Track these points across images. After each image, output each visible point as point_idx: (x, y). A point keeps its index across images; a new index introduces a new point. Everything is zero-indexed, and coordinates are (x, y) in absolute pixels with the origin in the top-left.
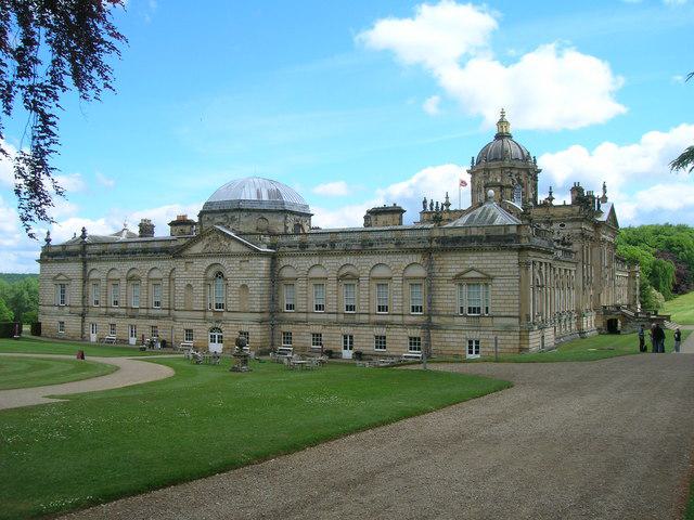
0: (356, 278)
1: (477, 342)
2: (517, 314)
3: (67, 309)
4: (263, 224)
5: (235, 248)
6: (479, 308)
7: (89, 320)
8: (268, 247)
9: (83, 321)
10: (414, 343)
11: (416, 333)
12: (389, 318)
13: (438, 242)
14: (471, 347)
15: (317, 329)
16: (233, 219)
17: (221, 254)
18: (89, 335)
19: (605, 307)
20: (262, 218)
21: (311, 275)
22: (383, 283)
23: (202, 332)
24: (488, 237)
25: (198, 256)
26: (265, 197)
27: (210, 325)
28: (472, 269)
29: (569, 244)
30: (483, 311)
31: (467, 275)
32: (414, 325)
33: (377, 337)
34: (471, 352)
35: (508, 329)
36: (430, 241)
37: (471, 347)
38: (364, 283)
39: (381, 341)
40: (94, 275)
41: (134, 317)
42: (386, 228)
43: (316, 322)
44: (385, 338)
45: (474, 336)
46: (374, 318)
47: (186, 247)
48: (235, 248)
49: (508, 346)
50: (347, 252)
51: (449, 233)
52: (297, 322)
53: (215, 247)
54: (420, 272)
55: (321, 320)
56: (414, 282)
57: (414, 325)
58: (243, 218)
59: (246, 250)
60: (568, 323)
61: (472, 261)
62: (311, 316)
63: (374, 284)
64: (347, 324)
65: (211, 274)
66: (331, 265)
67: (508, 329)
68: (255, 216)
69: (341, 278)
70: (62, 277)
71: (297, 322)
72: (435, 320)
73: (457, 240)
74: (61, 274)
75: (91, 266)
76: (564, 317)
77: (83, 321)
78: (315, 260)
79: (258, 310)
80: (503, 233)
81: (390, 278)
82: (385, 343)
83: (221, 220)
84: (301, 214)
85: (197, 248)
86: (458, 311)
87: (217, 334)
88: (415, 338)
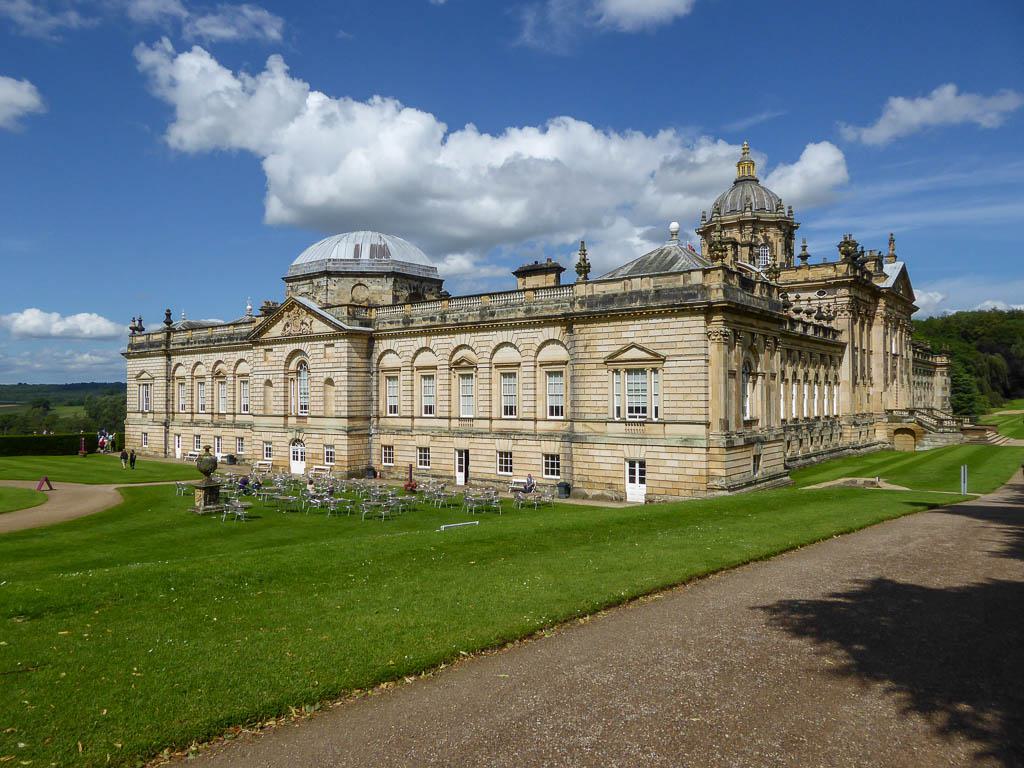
0: (472, 366)
1: (642, 464)
2: (702, 418)
3: (150, 416)
4: (362, 294)
5: (319, 327)
6: (644, 410)
7: (174, 429)
8: (361, 325)
9: (167, 432)
10: (552, 462)
11: (553, 447)
12: (518, 425)
13: (582, 304)
15: (424, 441)
18: (174, 450)
19: (891, 411)
21: (417, 363)
22: (509, 371)
23: (281, 442)
24: (657, 291)
25: (276, 341)
26: (365, 255)
27: (290, 436)
28: (634, 346)
29: (830, 319)
30: (650, 414)
31: (620, 357)
32: (550, 436)
33: (501, 454)
35: (687, 443)
36: (572, 304)
37: (632, 472)
38: (483, 372)
39: (506, 460)
40: (180, 372)
41: (217, 425)
43: (423, 431)
44: (511, 454)
45: (638, 453)
46: (497, 425)
47: (264, 329)
48: (319, 327)
49: (688, 471)
52: (399, 431)
53: (293, 330)
54: (555, 353)
55: (432, 429)
56: (554, 370)
57: (550, 436)
58: (334, 285)
60: (826, 434)
61: (633, 331)
62: (417, 422)
63: (496, 373)
65: (293, 366)
66: (443, 344)
67: (687, 443)
68: (349, 282)
69: (457, 365)
70: (144, 376)
71: (399, 431)
72: (579, 428)
73: (610, 299)
74: (143, 372)
75: (176, 359)
76: (819, 425)
77: (167, 432)
78: (421, 342)
79: (345, 414)
80: (680, 284)
81: (519, 365)
83: (305, 289)
84: (422, 280)
85: (276, 331)
86: (612, 414)
87: (299, 448)
88: (553, 457)
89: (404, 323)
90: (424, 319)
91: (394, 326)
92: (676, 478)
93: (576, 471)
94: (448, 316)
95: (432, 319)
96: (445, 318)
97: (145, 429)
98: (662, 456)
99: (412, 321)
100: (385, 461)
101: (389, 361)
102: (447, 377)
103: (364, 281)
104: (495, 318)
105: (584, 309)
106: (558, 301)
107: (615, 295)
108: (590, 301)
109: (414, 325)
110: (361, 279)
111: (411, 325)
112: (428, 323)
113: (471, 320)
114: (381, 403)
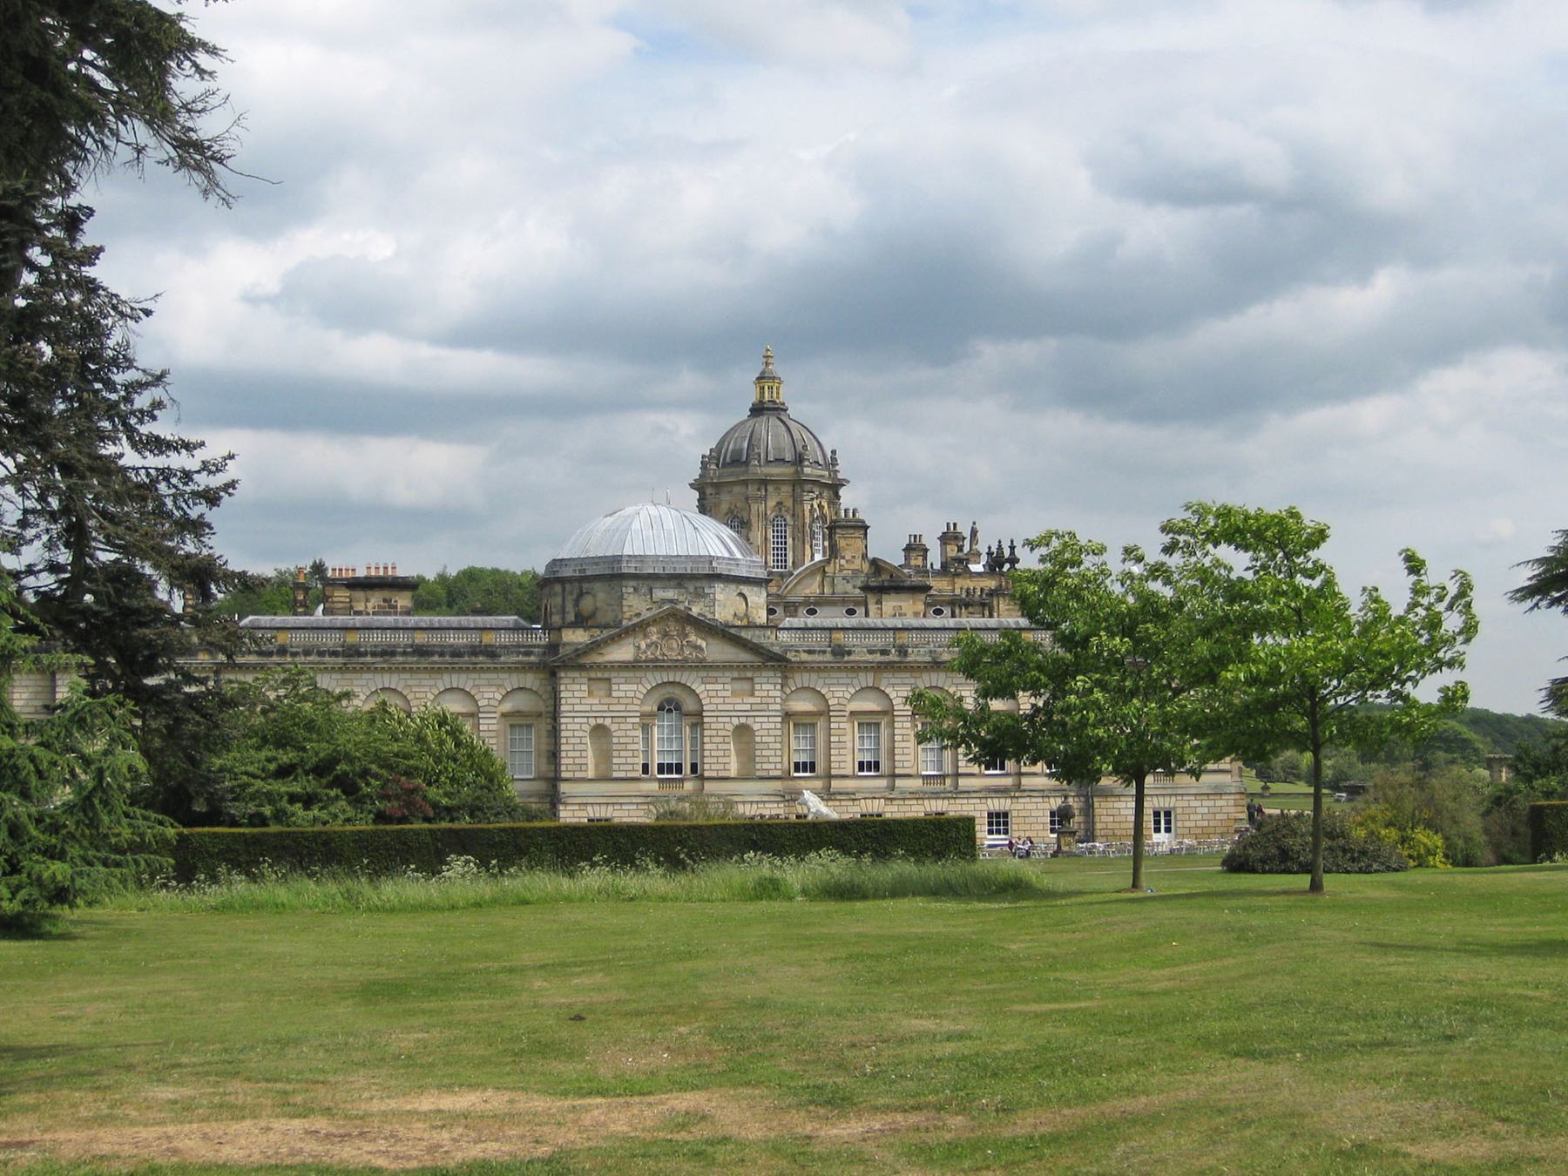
1: (1168, 814)
14: (1157, 822)
17: (682, 665)
34: (1157, 830)
37: (1157, 822)
47: (595, 646)
48: (715, 650)
64: (936, 795)
82: (1006, 823)
83: (670, 594)
85: (623, 652)
89: (834, 653)
90: (871, 652)
91: (816, 657)
92: (1205, 823)
93: (1098, 826)
95: (884, 652)
96: (906, 654)
98: (1194, 804)
99: (849, 653)
101: (802, 705)
103: (745, 589)
109: (852, 658)
112: (878, 658)
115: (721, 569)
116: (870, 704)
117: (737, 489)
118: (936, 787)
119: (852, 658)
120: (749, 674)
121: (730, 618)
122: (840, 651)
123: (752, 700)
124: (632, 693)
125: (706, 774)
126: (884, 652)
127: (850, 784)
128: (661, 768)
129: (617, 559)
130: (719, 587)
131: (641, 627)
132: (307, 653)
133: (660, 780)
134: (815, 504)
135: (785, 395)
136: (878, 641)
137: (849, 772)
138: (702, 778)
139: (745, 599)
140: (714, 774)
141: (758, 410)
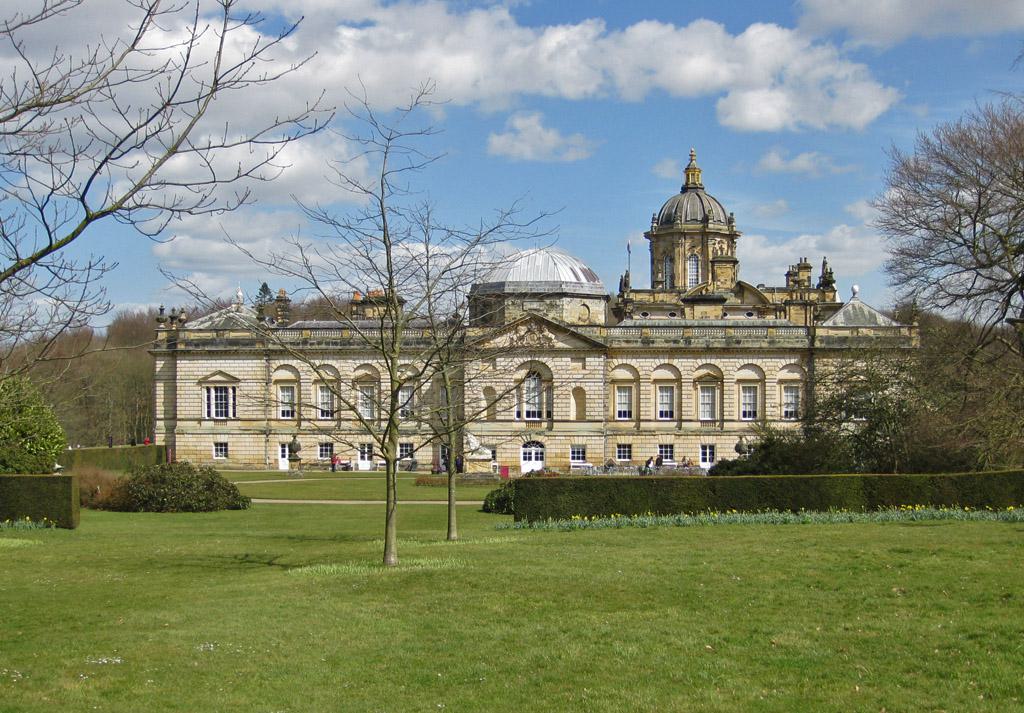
13: (821, 341)
15: (668, 440)
16: (552, 306)
17: (541, 351)
20: (584, 305)
42: (707, 323)
50: (709, 351)
51: (832, 333)
59: (580, 344)
64: (708, 434)
71: (639, 432)
83: (535, 305)
85: (502, 341)
87: (533, 450)
89: (642, 342)
90: (667, 341)
94: (693, 340)
95: (675, 342)
96: (690, 343)
97: (222, 439)
99: (653, 342)
100: (620, 457)
102: (691, 388)
103: (587, 302)
104: (741, 346)
105: (823, 345)
106: (797, 337)
107: (847, 338)
108: (827, 339)
109: (655, 345)
110: (585, 300)
111: (651, 345)
112: (672, 345)
113: (716, 345)
114: (611, 409)
115: (566, 289)
116: (667, 374)
117: (668, 238)
118: (710, 428)
119: (655, 345)
120: (582, 356)
121: (575, 320)
122: (647, 341)
123: (584, 372)
124: (511, 369)
125: (555, 418)
126: (675, 342)
127: (653, 425)
128: (528, 414)
129: (502, 284)
130: (566, 300)
131: (514, 326)
132: (319, 343)
133: (526, 422)
134: (717, 246)
135: (701, 180)
136: (673, 334)
137: (653, 418)
138: (553, 421)
139: (588, 308)
140: (560, 418)
141: (685, 190)
